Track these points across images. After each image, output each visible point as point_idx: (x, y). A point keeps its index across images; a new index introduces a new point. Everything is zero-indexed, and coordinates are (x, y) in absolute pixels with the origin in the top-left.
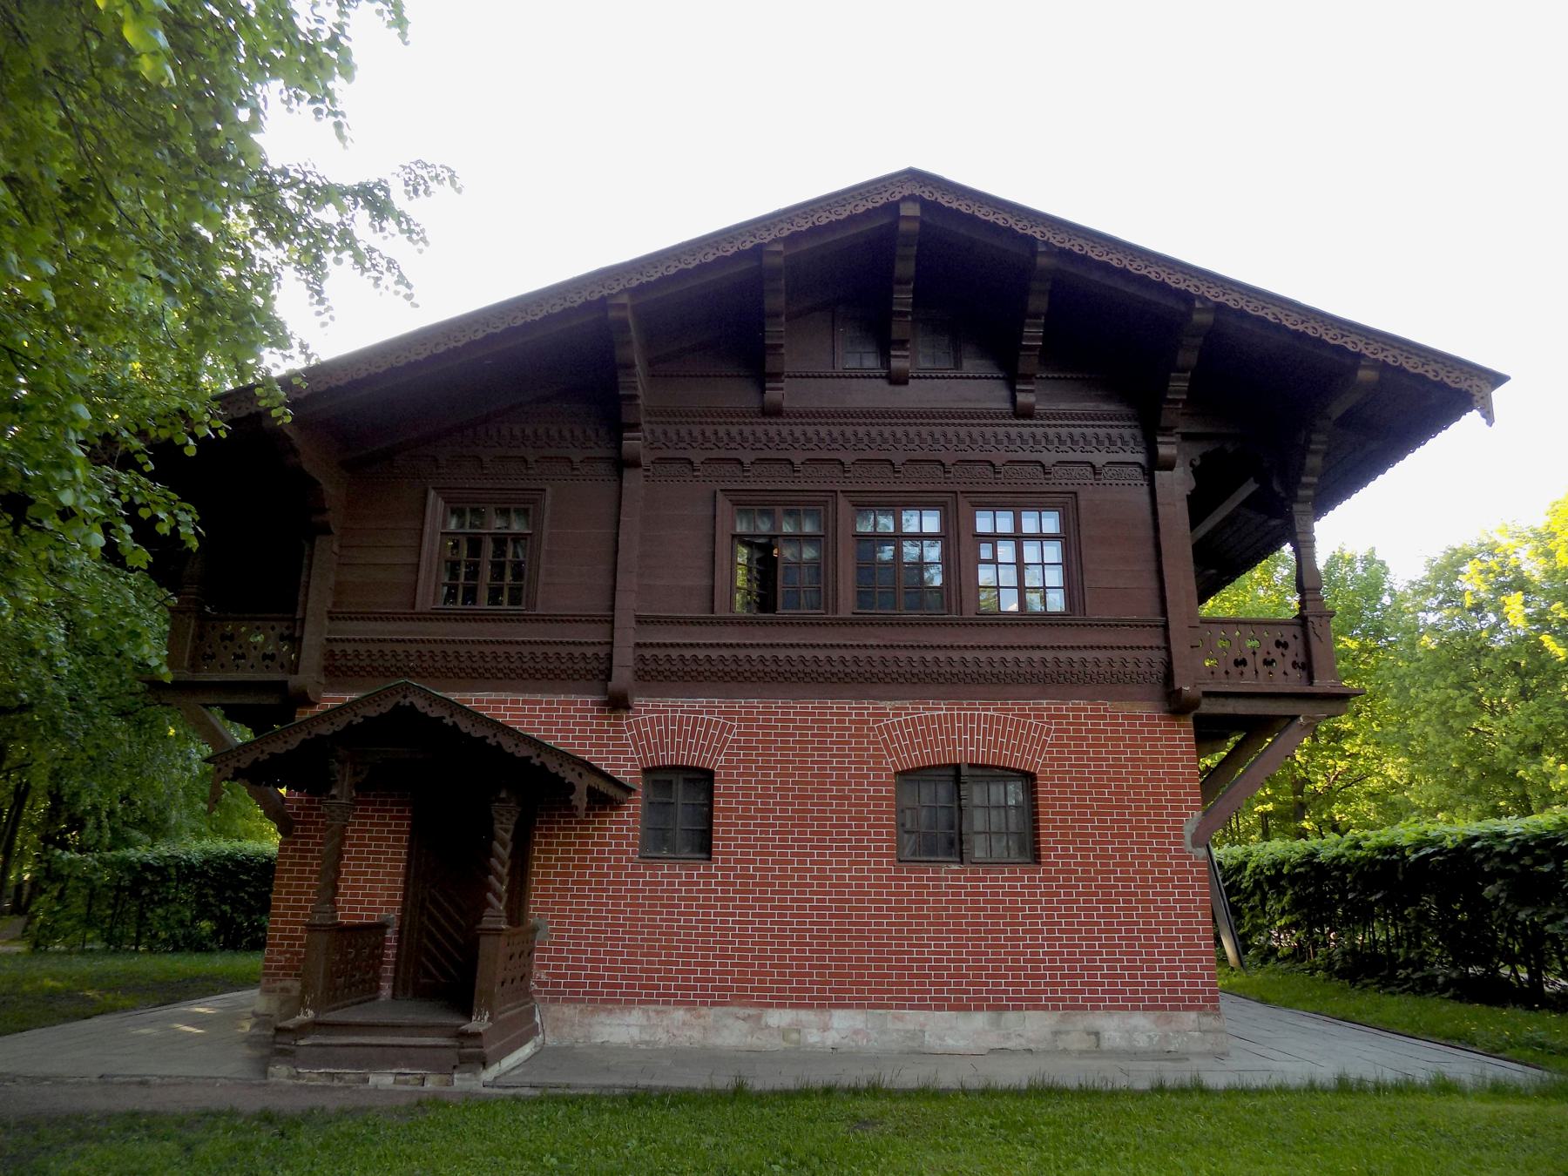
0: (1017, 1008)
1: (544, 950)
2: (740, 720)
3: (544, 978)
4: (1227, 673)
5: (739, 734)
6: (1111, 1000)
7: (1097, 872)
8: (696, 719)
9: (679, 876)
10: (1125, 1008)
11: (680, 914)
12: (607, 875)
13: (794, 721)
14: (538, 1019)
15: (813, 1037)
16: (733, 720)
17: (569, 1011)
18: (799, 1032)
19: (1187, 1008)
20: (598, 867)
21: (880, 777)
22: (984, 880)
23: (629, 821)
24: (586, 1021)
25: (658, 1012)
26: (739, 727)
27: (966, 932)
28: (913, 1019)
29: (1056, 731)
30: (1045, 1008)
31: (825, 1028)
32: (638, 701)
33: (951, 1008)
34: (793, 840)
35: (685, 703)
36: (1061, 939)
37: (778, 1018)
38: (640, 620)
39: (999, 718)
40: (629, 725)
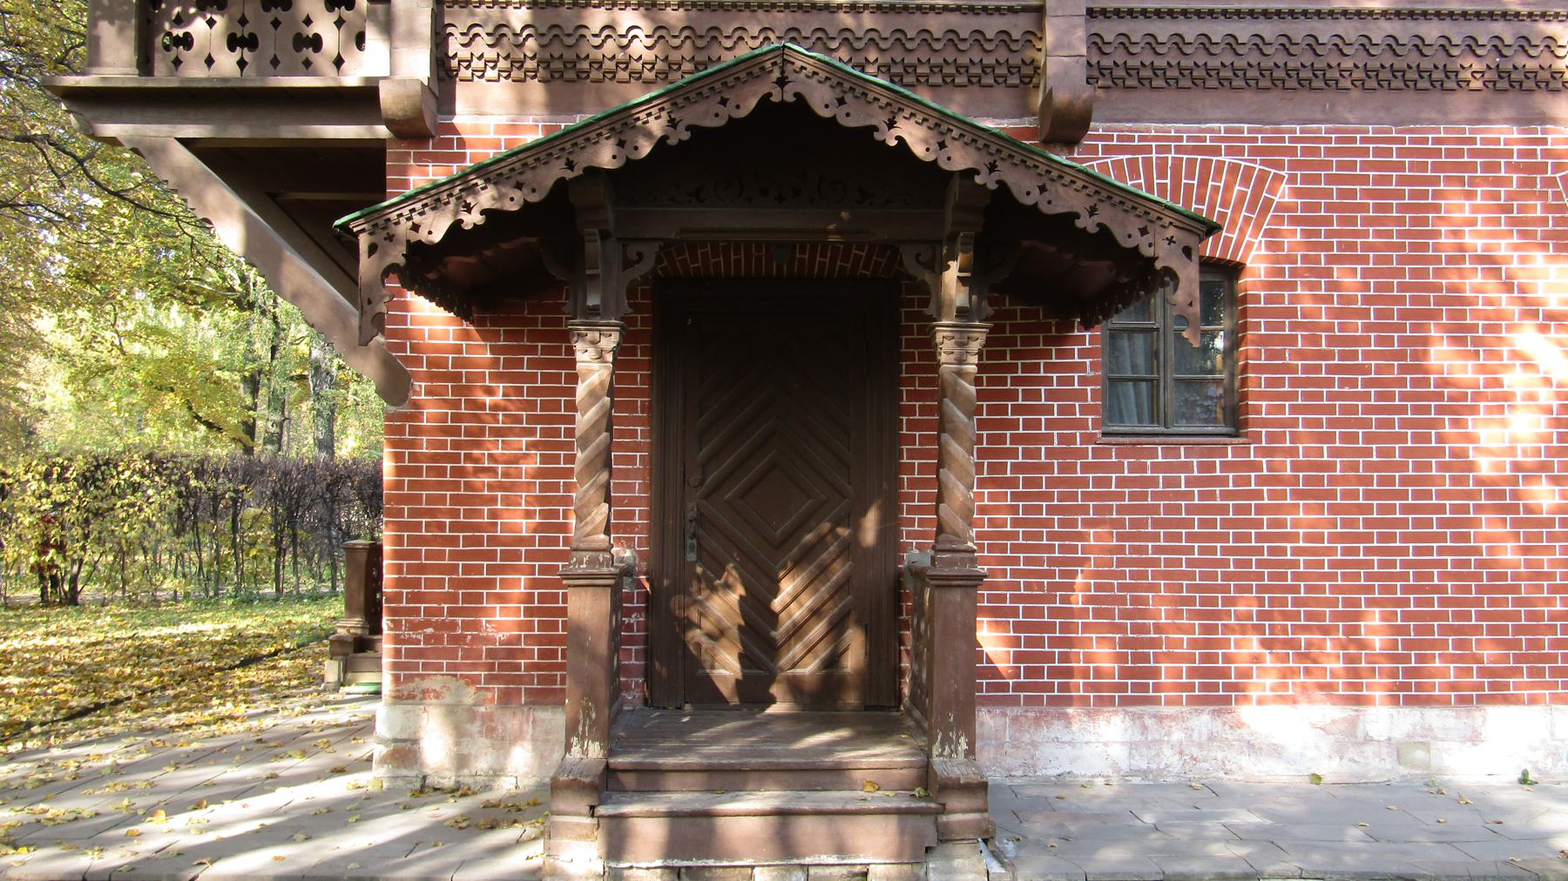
2: (1294, 165)
8: (1206, 164)
9: (1186, 467)
12: (1047, 468)
13: (1399, 166)
16: (1279, 165)
18: (1425, 746)
24: (1026, 738)
25: (1160, 718)
26: (1292, 179)
34: (1404, 396)
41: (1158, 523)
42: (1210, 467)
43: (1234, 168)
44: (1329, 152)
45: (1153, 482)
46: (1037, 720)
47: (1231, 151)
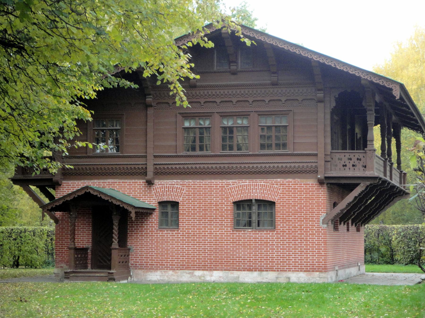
0: (267, 271)
1: (133, 255)
2: (186, 187)
3: (133, 263)
4: (340, 169)
5: (186, 191)
6: (294, 269)
7: (292, 232)
8: (173, 187)
9: (170, 233)
10: (298, 271)
11: (170, 244)
12: (149, 233)
14: (131, 274)
15: (208, 278)
16: (184, 187)
17: (140, 272)
19: (316, 271)
20: (146, 231)
21: (228, 203)
22: (258, 234)
23: (155, 218)
25: (165, 272)
26: (186, 189)
27: (252, 249)
28: (236, 274)
29: (282, 189)
30: (275, 271)
31: (211, 276)
32: (156, 182)
33: (247, 271)
34: (202, 223)
35: (170, 182)
36: (280, 251)
37: (198, 273)
38: (155, 157)
39: (265, 185)
40: (153, 189)
41: (165, 242)
42: (173, 233)
43: (177, 187)
44: (192, 184)
45: (165, 236)
46: (147, 272)
47: (177, 185)
